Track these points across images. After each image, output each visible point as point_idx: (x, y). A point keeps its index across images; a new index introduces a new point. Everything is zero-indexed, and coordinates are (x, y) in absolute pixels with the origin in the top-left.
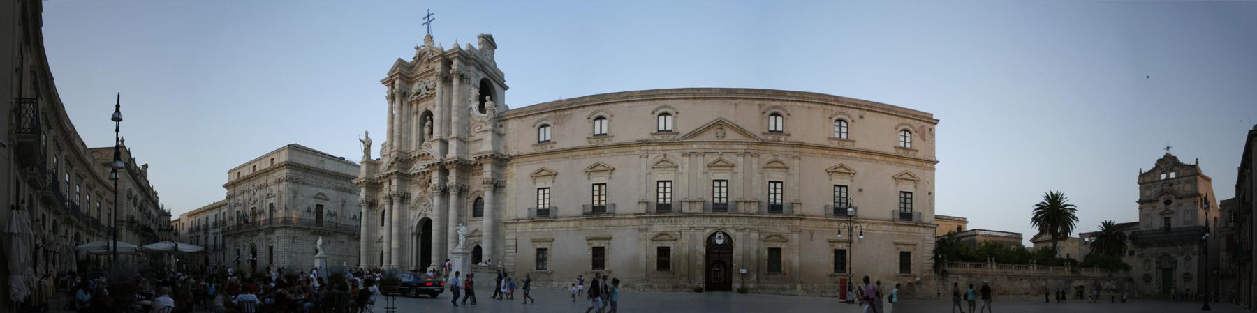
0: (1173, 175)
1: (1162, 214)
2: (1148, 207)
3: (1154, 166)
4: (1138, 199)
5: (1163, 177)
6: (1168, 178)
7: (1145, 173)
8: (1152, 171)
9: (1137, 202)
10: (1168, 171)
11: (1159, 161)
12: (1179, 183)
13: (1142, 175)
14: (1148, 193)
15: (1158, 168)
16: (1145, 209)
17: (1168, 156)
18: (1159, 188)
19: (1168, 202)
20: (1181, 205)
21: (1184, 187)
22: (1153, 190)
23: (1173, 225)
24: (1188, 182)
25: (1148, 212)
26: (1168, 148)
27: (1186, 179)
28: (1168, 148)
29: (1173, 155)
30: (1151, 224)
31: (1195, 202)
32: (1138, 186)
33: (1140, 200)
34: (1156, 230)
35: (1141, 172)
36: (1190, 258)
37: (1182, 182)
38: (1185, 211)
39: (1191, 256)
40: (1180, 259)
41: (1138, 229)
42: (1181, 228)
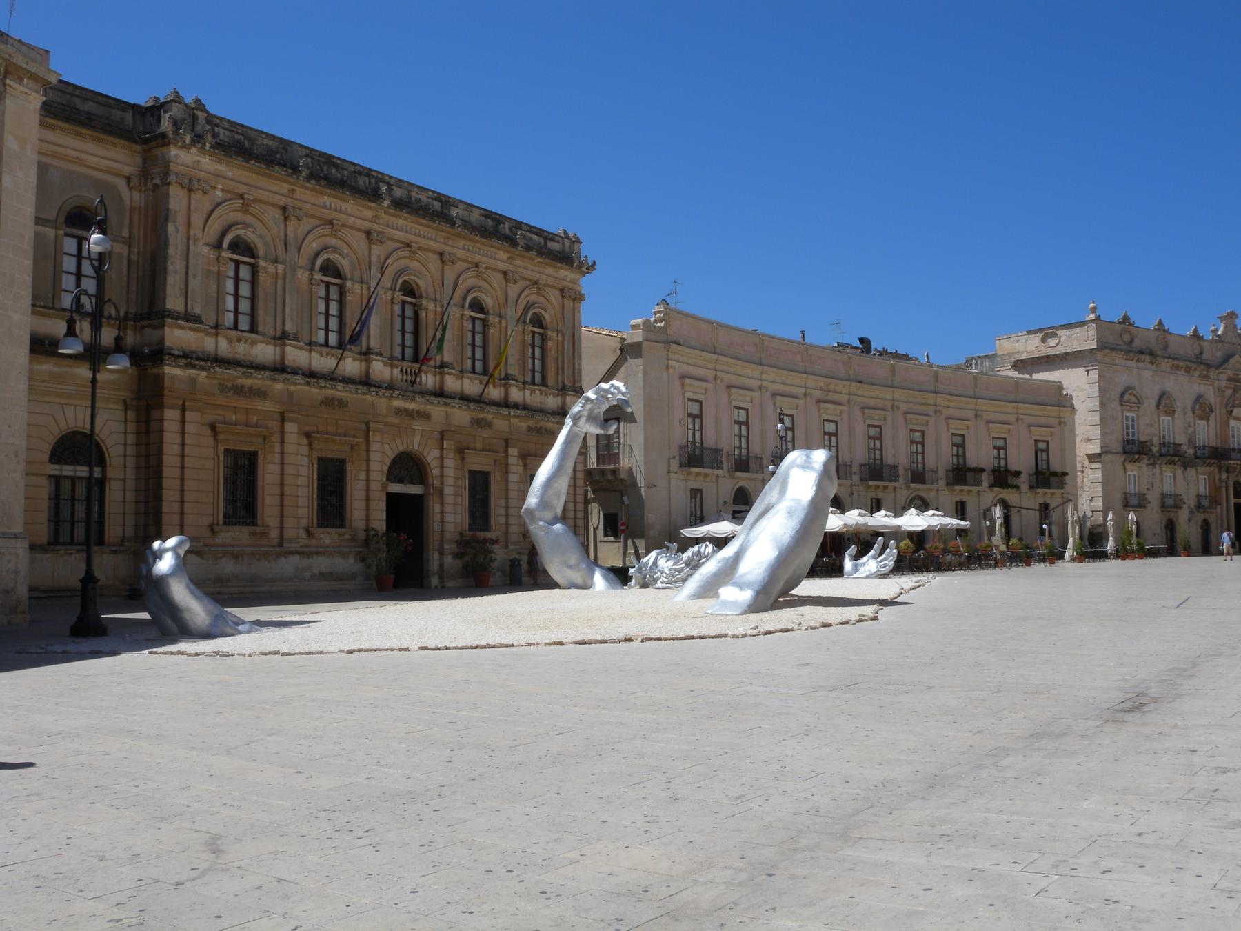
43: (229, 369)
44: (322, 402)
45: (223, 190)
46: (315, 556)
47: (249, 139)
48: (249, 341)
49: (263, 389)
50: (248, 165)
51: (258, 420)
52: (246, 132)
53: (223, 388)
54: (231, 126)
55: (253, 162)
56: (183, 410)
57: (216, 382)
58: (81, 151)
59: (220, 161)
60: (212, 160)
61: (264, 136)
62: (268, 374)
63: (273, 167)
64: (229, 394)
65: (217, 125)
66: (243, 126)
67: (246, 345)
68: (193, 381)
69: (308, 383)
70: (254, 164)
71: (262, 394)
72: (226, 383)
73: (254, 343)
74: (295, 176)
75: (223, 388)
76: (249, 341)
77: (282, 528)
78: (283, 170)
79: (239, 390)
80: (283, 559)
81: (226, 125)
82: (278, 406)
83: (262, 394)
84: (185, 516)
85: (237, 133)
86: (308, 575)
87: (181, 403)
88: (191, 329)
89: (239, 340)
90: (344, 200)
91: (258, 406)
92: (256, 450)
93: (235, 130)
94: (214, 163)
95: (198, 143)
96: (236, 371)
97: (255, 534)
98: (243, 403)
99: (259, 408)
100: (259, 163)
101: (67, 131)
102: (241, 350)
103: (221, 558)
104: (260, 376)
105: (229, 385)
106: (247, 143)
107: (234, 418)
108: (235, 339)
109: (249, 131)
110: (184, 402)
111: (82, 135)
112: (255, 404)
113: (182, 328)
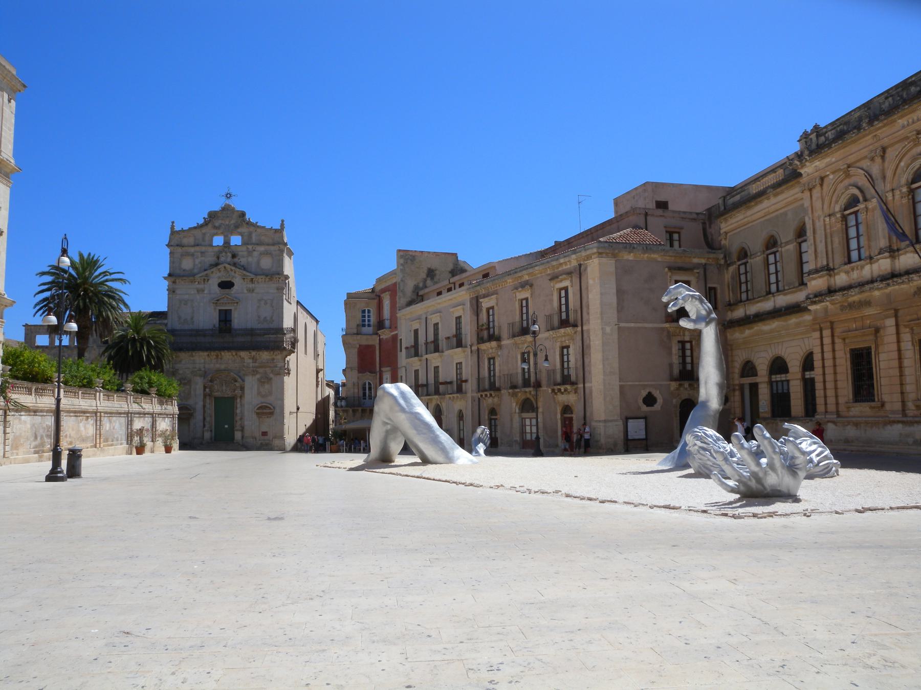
0: (236, 240)
1: (217, 302)
2: (186, 290)
3: (201, 221)
4: (166, 272)
5: (218, 241)
6: (227, 243)
7: (182, 231)
8: (199, 227)
9: (165, 278)
10: (228, 232)
11: (212, 215)
12: (250, 253)
13: (173, 233)
14: (187, 264)
15: (210, 225)
16: (178, 292)
17: (227, 209)
18: (211, 259)
19: (226, 285)
20: (251, 291)
21: (258, 263)
22: (197, 261)
23: (238, 320)
24: (266, 253)
25: (186, 297)
26: (228, 196)
27: (262, 248)
28: (228, 196)
29: (239, 208)
30: (192, 318)
31: (278, 289)
32: (168, 250)
33: (170, 275)
34: (203, 330)
35: (172, 227)
36: (271, 379)
37: (255, 254)
38: (260, 300)
39: (271, 376)
40: (251, 383)
41: (166, 325)
42: (252, 330)
43: (833, 296)
44: (915, 293)
45: (833, 173)
46: (916, 425)
47: (845, 123)
48: (859, 267)
49: (868, 300)
50: (833, 149)
51: (870, 322)
52: (842, 121)
53: (843, 308)
54: (833, 125)
55: (833, 145)
56: (821, 330)
57: (838, 306)
58: (793, 195)
59: (823, 158)
60: (819, 161)
61: (853, 113)
62: (857, 290)
63: (845, 138)
64: (847, 311)
65: (826, 132)
66: (837, 120)
67: (858, 271)
68: (826, 309)
69: (888, 285)
70: (835, 146)
71: (867, 303)
72: (844, 304)
73: (862, 267)
74: (862, 130)
75: (843, 308)
76: (859, 267)
77: (826, 404)
78: (852, 134)
79: (852, 306)
80: (889, 427)
81: (830, 128)
82: (879, 309)
83: (867, 303)
84: (828, 398)
85: (838, 126)
86: (910, 440)
87: (818, 326)
88: (820, 277)
89: (853, 270)
90: (914, 111)
91: (865, 313)
92: (869, 345)
93: (835, 126)
94: (823, 161)
95: (803, 160)
96: (838, 295)
97: (874, 408)
98: (856, 314)
99: (867, 314)
100: (836, 142)
101: (787, 189)
102: (855, 276)
103: (847, 425)
104: (853, 293)
105: (846, 304)
106: (845, 128)
107: (854, 326)
108: (850, 270)
109: (843, 119)
110: (820, 326)
111: (792, 186)
112: (863, 312)
113: (814, 279)
